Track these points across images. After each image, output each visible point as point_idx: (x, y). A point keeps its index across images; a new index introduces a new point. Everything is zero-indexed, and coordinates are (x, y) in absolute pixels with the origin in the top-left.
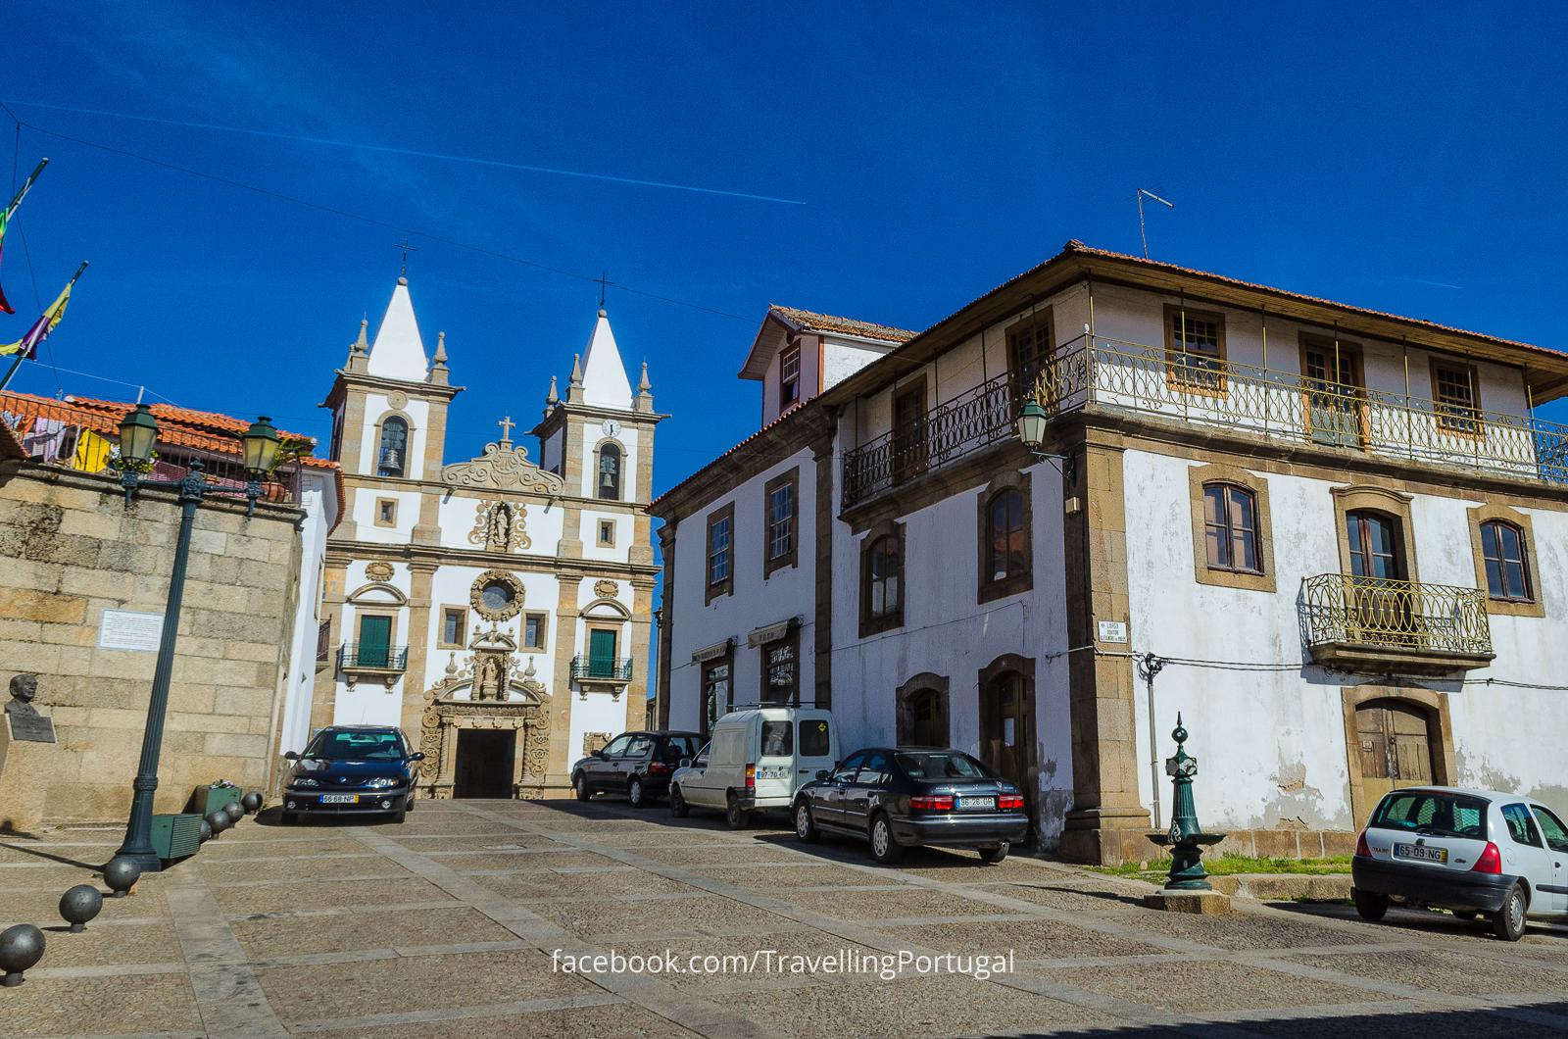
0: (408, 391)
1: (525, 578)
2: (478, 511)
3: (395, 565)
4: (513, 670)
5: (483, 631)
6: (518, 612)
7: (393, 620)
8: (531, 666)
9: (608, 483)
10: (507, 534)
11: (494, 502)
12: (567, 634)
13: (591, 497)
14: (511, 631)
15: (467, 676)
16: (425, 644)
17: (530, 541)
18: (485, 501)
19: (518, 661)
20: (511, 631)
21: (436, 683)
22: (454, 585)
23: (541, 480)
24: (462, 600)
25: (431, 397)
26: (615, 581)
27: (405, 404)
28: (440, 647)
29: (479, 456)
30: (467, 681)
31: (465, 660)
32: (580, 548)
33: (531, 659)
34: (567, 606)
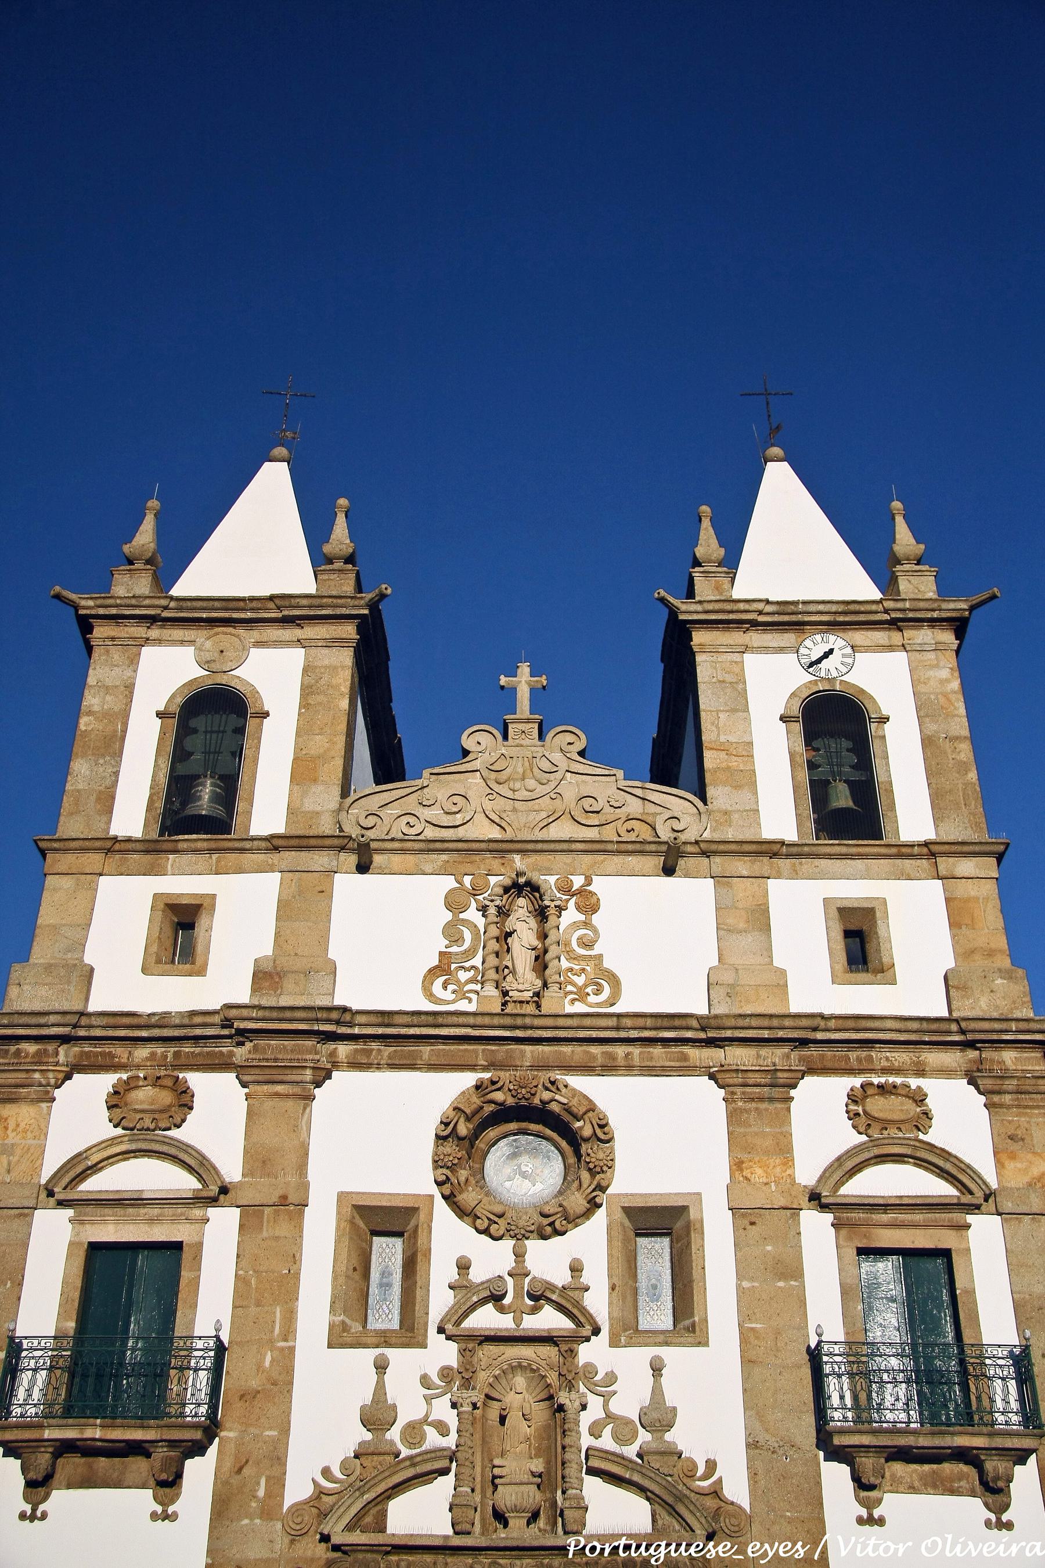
1: (612, 1095)
2: (449, 906)
3: (194, 1079)
4: (595, 1410)
5: (477, 1275)
7: (186, 1255)
8: (657, 1392)
9: (842, 798)
11: (493, 880)
12: (775, 1273)
13: (789, 833)
14: (576, 1269)
15: (433, 1439)
16: (289, 1331)
17: (615, 982)
18: (467, 880)
19: (611, 1378)
20: (576, 1269)
21: (326, 1472)
22: (377, 1129)
23: (634, 807)
24: (407, 1171)
25: (310, 631)
26: (914, 1082)
28: (339, 1338)
29: (451, 761)
30: (436, 1453)
31: (425, 1381)
32: (780, 985)
33: (657, 1369)
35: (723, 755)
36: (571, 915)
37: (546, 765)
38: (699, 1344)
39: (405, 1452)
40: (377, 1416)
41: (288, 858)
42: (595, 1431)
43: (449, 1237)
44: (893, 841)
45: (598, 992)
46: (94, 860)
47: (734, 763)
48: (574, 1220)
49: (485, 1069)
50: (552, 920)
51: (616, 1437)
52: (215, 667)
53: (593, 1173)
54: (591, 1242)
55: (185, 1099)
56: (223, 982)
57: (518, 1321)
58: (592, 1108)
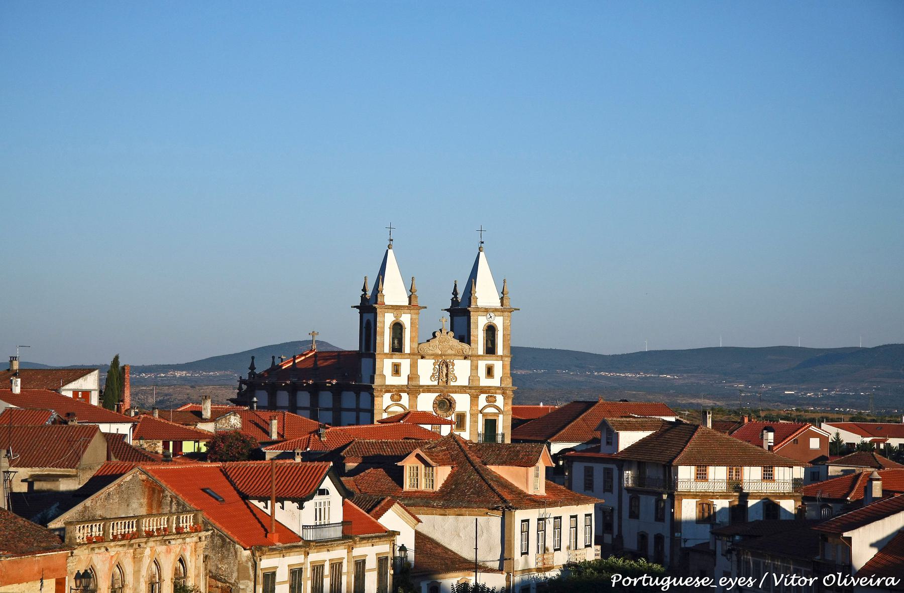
3: (402, 394)
10: (447, 375)
12: (474, 422)
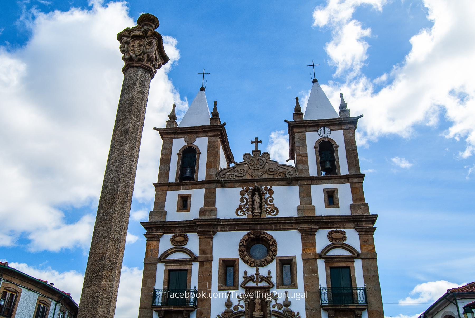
0: (196, 133)
3: (188, 235)
5: (249, 275)
6: (273, 259)
8: (287, 298)
10: (260, 207)
11: (250, 188)
12: (311, 273)
13: (316, 175)
14: (269, 273)
17: (277, 210)
18: (245, 188)
19: (277, 296)
20: (269, 273)
25: (209, 134)
26: (343, 230)
27: (194, 141)
28: (220, 289)
30: (241, 312)
34: (308, 251)
35: (301, 157)
36: (268, 195)
37: (261, 161)
38: (295, 288)
39: (234, 312)
40: (228, 304)
41: (206, 185)
42: (274, 307)
43: (243, 267)
44: (339, 175)
45: (273, 212)
46: (166, 188)
47: (303, 158)
48: (269, 262)
49: (249, 230)
50: (263, 197)
51: (279, 308)
52: (189, 143)
53: (272, 252)
54: (272, 267)
55: (187, 239)
56: (194, 213)
57: (257, 284)
58: (272, 238)
